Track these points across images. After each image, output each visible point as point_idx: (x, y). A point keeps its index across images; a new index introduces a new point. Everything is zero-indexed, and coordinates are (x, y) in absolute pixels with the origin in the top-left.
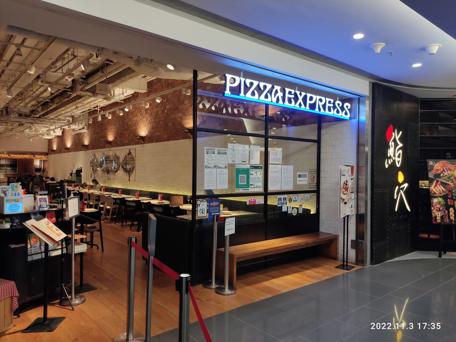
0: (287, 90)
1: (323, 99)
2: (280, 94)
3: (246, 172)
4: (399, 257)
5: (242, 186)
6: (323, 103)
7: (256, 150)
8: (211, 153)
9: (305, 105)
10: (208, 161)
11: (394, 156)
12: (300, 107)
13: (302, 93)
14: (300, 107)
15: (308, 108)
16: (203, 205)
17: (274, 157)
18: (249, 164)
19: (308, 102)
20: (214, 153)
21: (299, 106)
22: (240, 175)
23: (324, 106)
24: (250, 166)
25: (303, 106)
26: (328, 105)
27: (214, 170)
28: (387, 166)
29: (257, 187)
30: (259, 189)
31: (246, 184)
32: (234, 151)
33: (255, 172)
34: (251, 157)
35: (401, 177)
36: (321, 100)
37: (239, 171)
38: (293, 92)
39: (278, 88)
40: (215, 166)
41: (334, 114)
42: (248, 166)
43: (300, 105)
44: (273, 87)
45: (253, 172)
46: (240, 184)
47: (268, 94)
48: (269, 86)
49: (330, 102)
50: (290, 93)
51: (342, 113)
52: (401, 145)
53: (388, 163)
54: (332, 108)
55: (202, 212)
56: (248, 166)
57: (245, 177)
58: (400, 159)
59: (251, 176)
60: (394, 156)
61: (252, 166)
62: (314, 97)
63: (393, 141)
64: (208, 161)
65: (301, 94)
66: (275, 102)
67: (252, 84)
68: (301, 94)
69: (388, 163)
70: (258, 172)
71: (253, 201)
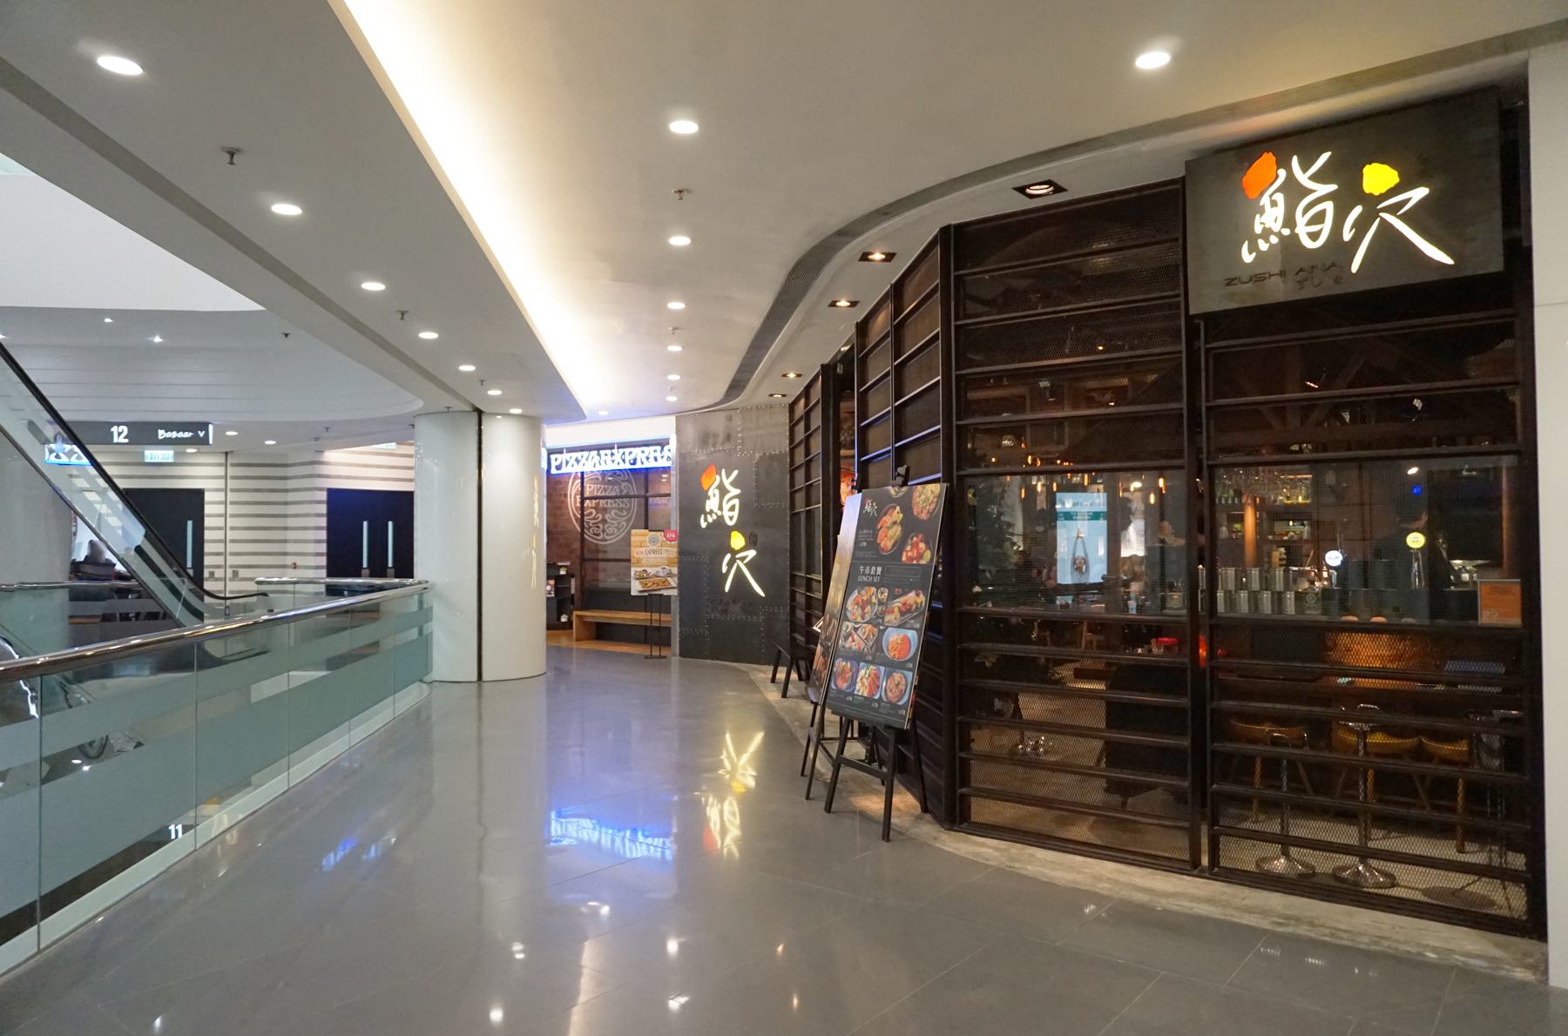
6: (646, 454)
11: (721, 508)
28: (704, 525)
35: (737, 540)
47: (586, 462)
52: (736, 491)
53: (706, 520)
58: (736, 514)
60: (721, 508)
63: (718, 487)
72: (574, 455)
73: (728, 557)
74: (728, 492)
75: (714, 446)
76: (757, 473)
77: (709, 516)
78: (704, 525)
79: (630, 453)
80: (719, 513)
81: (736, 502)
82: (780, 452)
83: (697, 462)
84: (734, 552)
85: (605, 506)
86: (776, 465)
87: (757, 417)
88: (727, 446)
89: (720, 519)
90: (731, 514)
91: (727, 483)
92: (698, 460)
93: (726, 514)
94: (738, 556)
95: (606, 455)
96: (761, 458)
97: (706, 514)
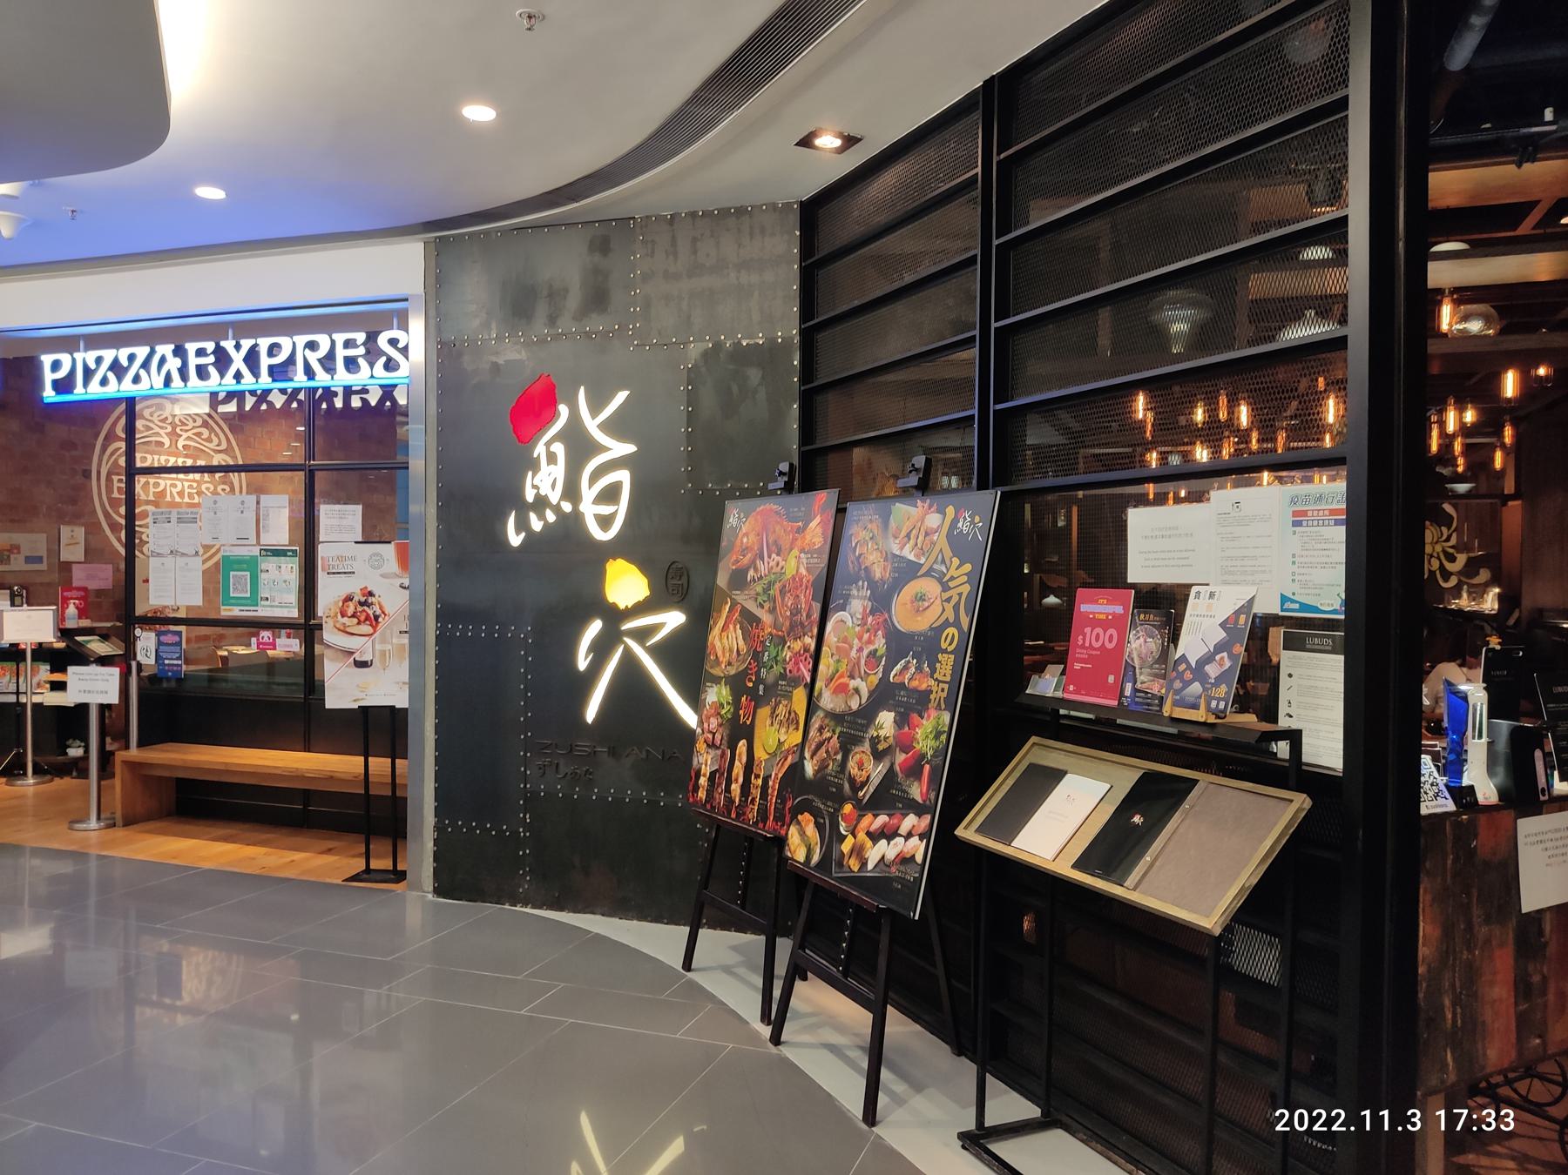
0: (192, 348)
1: (323, 341)
2: (173, 364)
3: (251, 565)
4: (615, 921)
5: (239, 602)
7: (279, 507)
8: (164, 522)
9: (256, 373)
10: (1303, 571)
11: (571, 491)
12: (238, 382)
13: (243, 342)
14: (238, 382)
15: (265, 381)
16: (148, 639)
17: (335, 522)
18: (258, 543)
19: (265, 362)
20: (169, 522)
21: (235, 381)
22: (232, 573)
23: (328, 362)
24: (261, 550)
25: (248, 377)
26: (341, 353)
27: (169, 560)
29: (280, 606)
30: (289, 612)
31: (249, 595)
32: (215, 513)
33: (275, 565)
34: (263, 527)
36: (312, 346)
37: (231, 563)
38: (210, 346)
39: (165, 349)
40: (172, 552)
41: (372, 377)
42: (256, 551)
43: (238, 376)
44: (152, 353)
45: (270, 564)
46: (232, 595)
47: (143, 373)
48: (142, 352)
49: (348, 344)
50: (201, 353)
51: (372, 368)
54: (212, 370)
55: (146, 655)
56: (256, 551)
57: (246, 579)
59: (264, 576)
60: (571, 491)
61: (265, 550)
62: (286, 342)
64: (1303, 571)
65: (238, 347)
66: (162, 386)
67: (99, 360)
68: (238, 347)
69: (120, 516)
70: (283, 566)
71: (268, 641)
72: (108, 355)
73: (595, 627)
74: (600, 449)
75: (552, 320)
76: (692, 398)
77: (533, 516)
78: (515, 540)
79: (273, 349)
80: (567, 507)
81: (623, 476)
82: (772, 341)
83: (496, 368)
84: (614, 616)
85: (178, 499)
86: (754, 375)
87: (695, 240)
88: (597, 323)
89: (571, 526)
90: (606, 510)
91: (592, 425)
92: (501, 361)
93: (589, 509)
94: (628, 625)
95: (201, 353)
96: (706, 354)
97: (523, 508)
